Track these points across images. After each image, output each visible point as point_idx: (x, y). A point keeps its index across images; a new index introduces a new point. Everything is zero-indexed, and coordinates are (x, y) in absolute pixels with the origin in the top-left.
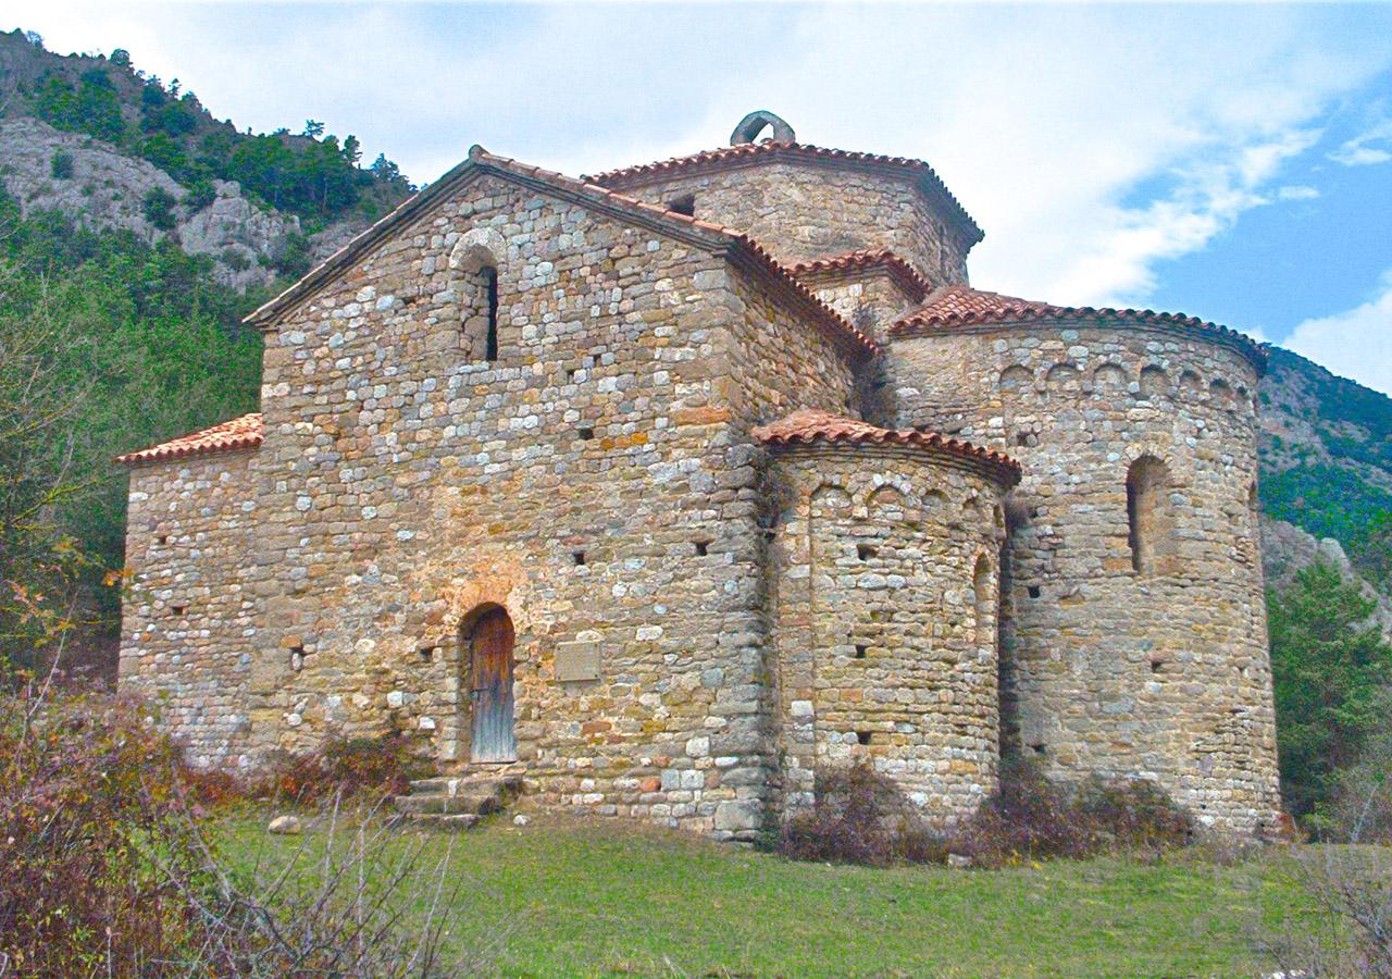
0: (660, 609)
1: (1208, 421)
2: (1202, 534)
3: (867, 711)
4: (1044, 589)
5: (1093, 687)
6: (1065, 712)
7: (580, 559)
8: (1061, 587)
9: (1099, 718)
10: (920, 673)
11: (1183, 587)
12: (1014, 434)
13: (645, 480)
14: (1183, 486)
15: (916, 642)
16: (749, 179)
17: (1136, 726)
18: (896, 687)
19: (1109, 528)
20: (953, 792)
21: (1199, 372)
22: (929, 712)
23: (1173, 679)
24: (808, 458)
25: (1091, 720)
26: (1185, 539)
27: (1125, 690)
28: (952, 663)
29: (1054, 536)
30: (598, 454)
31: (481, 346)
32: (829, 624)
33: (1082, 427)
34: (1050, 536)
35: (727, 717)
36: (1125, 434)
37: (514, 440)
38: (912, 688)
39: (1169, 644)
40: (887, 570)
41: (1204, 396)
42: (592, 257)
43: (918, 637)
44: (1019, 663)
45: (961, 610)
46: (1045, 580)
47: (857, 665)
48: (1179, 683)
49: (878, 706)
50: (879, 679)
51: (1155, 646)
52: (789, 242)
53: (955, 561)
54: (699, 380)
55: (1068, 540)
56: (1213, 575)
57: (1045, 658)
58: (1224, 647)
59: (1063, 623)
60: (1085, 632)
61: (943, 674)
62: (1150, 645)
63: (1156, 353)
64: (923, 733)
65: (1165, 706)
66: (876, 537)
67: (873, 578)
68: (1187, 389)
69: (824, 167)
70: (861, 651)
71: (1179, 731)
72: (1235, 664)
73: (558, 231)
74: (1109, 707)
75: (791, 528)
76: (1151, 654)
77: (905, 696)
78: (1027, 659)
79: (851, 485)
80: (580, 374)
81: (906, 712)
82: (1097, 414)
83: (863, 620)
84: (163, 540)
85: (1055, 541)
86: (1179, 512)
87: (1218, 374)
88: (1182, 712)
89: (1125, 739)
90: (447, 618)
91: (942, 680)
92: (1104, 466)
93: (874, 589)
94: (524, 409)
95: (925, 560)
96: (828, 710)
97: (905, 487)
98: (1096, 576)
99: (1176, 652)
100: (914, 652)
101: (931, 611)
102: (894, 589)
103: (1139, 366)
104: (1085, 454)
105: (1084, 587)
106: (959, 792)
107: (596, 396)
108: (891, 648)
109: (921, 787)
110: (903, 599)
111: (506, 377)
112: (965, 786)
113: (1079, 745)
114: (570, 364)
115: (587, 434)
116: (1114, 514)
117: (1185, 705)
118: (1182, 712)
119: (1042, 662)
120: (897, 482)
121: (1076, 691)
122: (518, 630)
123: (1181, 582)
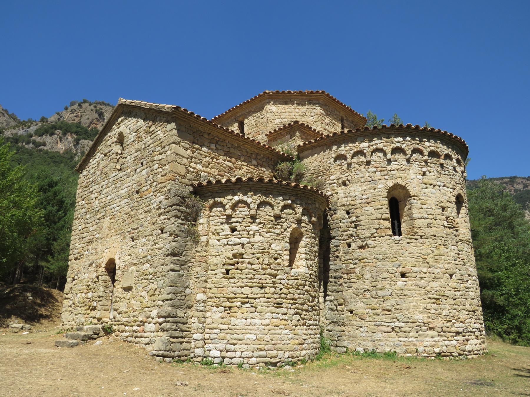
0: (149, 257)
1: (429, 168)
2: (426, 216)
3: (228, 298)
4: (353, 244)
5: (373, 284)
6: (361, 296)
8: (359, 243)
9: (376, 298)
10: (255, 280)
11: (417, 239)
12: (340, 181)
13: (150, 207)
14: (414, 196)
18: (242, 287)
19: (379, 216)
20: (272, 334)
21: (422, 148)
22: (259, 298)
25: (373, 299)
26: (416, 219)
27: (387, 286)
28: (275, 276)
29: (357, 221)
33: (367, 175)
34: (355, 222)
35: (163, 301)
36: (386, 177)
38: (251, 287)
39: (408, 265)
40: (240, 236)
41: (426, 158)
43: (254, 264)
44: (343, 275)
45: (281, 252)
46: (353, 240)
47: (225, 278)
49: (234, 296)
50: (235, 284)
52: (271, 125)
53: (278, 231)
56: (432, 233)
58: (440, 265)
60: (369, 261)
61: (268, 281)
62: (400, 266)
63: (399, 142)
66: (237, 222)
70: (228, 272)
71: (415, 304)
73: (137, 121)
75: (201, 221)
76: (400, 270)
77: (246, 290)
78: (346, 274)
81: (247, 298)
82: (374, 169)
83: (229, 258)
86: (413, 207)
88: (416, 295)
89: (389, 308)
91: (267, 283)
92: (377, 190)
95: (260, 231)
96: (212, 298)
97: (249, 200)
98: (375, 237)
99: (413, 269)
100: (252, 271)
103: (391, 147)
105: (369, 242)
106: (275, 334)
108: (241, 270)
109: (252, 332)
110: (248, 248)
112: (279, 331)
113: (367, 311)
114: (135, 168)
115: (138, 192)
117: (417, 292)
118: (416, 295)
119: (352, 275)
120: (245, 198)
121: (366, 287)
122: (117, 268)
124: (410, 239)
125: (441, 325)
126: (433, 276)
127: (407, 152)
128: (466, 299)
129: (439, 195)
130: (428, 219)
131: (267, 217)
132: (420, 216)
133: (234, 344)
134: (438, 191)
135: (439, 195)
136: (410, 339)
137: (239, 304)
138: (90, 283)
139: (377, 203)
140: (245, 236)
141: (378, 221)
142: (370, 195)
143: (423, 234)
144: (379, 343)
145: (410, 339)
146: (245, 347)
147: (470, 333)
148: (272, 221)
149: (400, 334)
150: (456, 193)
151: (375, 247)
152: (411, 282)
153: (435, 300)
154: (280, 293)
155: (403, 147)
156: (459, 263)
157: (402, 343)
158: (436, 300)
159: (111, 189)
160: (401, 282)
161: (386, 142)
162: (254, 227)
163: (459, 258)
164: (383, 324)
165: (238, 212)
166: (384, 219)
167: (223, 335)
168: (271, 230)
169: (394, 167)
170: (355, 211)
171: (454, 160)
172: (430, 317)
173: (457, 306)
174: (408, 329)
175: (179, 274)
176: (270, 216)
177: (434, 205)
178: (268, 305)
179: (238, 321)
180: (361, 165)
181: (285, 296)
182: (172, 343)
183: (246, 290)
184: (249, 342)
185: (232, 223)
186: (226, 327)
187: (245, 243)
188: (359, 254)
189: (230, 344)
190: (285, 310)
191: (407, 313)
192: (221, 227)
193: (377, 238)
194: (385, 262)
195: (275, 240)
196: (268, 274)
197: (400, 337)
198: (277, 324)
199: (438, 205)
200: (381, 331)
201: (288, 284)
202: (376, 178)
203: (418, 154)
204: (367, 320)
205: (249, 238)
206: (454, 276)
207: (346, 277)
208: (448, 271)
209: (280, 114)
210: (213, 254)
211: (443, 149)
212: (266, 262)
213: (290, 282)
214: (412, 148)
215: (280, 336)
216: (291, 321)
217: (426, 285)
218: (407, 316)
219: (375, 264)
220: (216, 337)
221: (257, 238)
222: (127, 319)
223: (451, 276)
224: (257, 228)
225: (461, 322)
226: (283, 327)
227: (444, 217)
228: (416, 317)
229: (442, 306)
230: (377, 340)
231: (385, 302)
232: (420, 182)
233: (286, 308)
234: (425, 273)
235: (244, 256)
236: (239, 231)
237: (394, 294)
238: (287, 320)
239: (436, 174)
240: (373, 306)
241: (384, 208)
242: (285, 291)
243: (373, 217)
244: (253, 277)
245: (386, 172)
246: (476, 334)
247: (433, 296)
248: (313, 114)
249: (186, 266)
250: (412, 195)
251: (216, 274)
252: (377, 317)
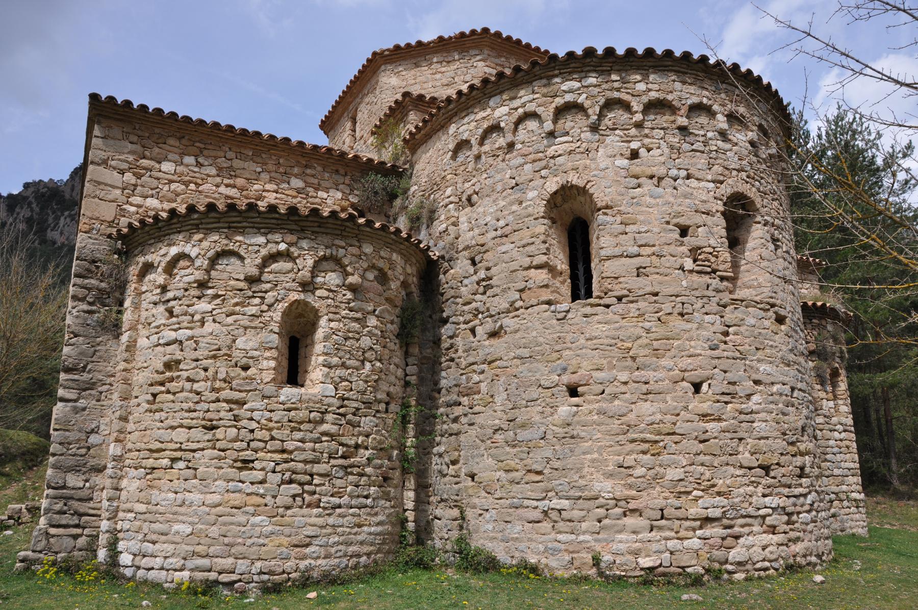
1: (647, 141)
2: (635, 250)
3: (151, 450)
4: (479, 330)
6: (489, 442)
8: (489, 325)
9: (514, 446)
11: (608, 306)
14: (607, 207)
15: (196, 386)
17: (549, 454)
18: (173, 428)
19: (526, 261)
20: (225, 524)
22: (203, 449)
23: (590, 402)
25: (508, 449)
26: (609, 258)
27: (537, 418)
28: (241, 403)
33: (508, 176)
34: (483, 280)
36: (543, 173)
39: (584, 367)
41: (638, 117)
43: (198, 381)
48: (596, 406)
49: (159, 445)
50: (162, 422)
53: (253, 310)
56: (649, 289)
57: (479, 392)
58: (665, 362)
59: (489, 358)
61: (222, 414)
62: (565, 369)
63: (571, 91)
64: (196, 469)
65: (577, 430)
66: (175, 299)
68: (616, 116)
71: (595, 456)
72: (683, 380)
74: (523, 435)
76: (566, 379)
77: (180, 435)
78: (467, 395)
81: (180, 449)
82: (520, 160)
87: (653, 95)
88: (599, 435)
89: (539, 468)
91: (221, 419)
92: (524, 205)
98: (517, 310)
99: (597, 375)
100: (191, 395)
102: (181, 341)
103: (554, 105)
105: (508, 322)
106: (232, 524)
108: (174, 394)
112: (242, 519)
113: (498, 473)
117: (603, 428)
118: (599, 435)
119: (476, 397)
120: (188, 249)
121: (497, 422)
123: (602, 302)
124: (592, 305)
125: (661, 502)
126: (644, 388)
127: (590, 111)
128: (741, 439)
129: (672, 199)
130: (639, 255)
131: (232, 282)
132: (618, 251)
133: (154, 543)
134: (669, 190)
135: (672, 199)
136: (581, 538)
137: (166, 462)
139: (526, 233)
140: (185, 324)
141: (525, 273)
142: (510, 218)
143: (625, 292)
144: (517, 544)
145: (581, 538)
146: (170, 548)
147: (748, 520)
148: (241, 290)
149: (561, 525)
150: (726, 190)
151: (516, 331)
152: (589, 405)
153: (646, 446)
154: (247, 440)
155: (579, 101)
156: (726, 354)
157: (563, 547)
158: (652, 446)
161: (544, 96)
162: (203, 306)
163: (725, 343)
165: (178, 278)
166: (538, 267)
168: (237, 308)
169: (560, 149)
170: (485, 256)
171: (720, 117)
172: (630, 487)
173: (708, 457)
174: (576, 514)
175: (75, 408)
176: (238, 280)
177: (656, 223)
178: (221, 463)
179: (164, 497)
180: (498, 156)
181: (261, 445)
182: (53, 536)
183: (180, 435)
184: (177, 539)
185: (168, 301)
186: (141, 508)
188: (487, 351)
189: (148, 542)
190: (259, 475)
191: (576, 477)
193: (522, 310)
195: (246, 328)
196: (228, 401)
197: (560, 532)
198: (236, 503)
199: (668, 223)
200: (520, 519)
201: (270, 420)
203: (621, 112)
204: (496, 496)
205: (191, 328)
206: (705, 387)
207: (466, 403)
208: (686, 374)
210: (140, 365)
211: (686, 93)
212: (221, 375)
213: (276, 416)
214: (603, 100)
215: (243, 529)
216: (274, 497)
217: (624, 410)
218: (576, 484)
219: (514, 371)
221: (209, 327)
223: (697, 387)
224: (209, 307)
225: (719, 494)
226: (251, 509)
227: (684, 249)
228: (597, 486)
229: (665, 458)
230: (512, 539)
231: (531, 455)
233: (263, 469)
234: (626, 383)
235: (181, 366)
237: (549, 436)
238: (262, 496)
239: (667, 151)
240: (507, 465)
241: (538, 241)
242: (265, 435)
243: (514, 265)
244: (193, 408)
245: (543, 163)
246: (769, 520)
247: (642, 436)
249: (93, 392)
250: (599, 205)
252: (515, 488)
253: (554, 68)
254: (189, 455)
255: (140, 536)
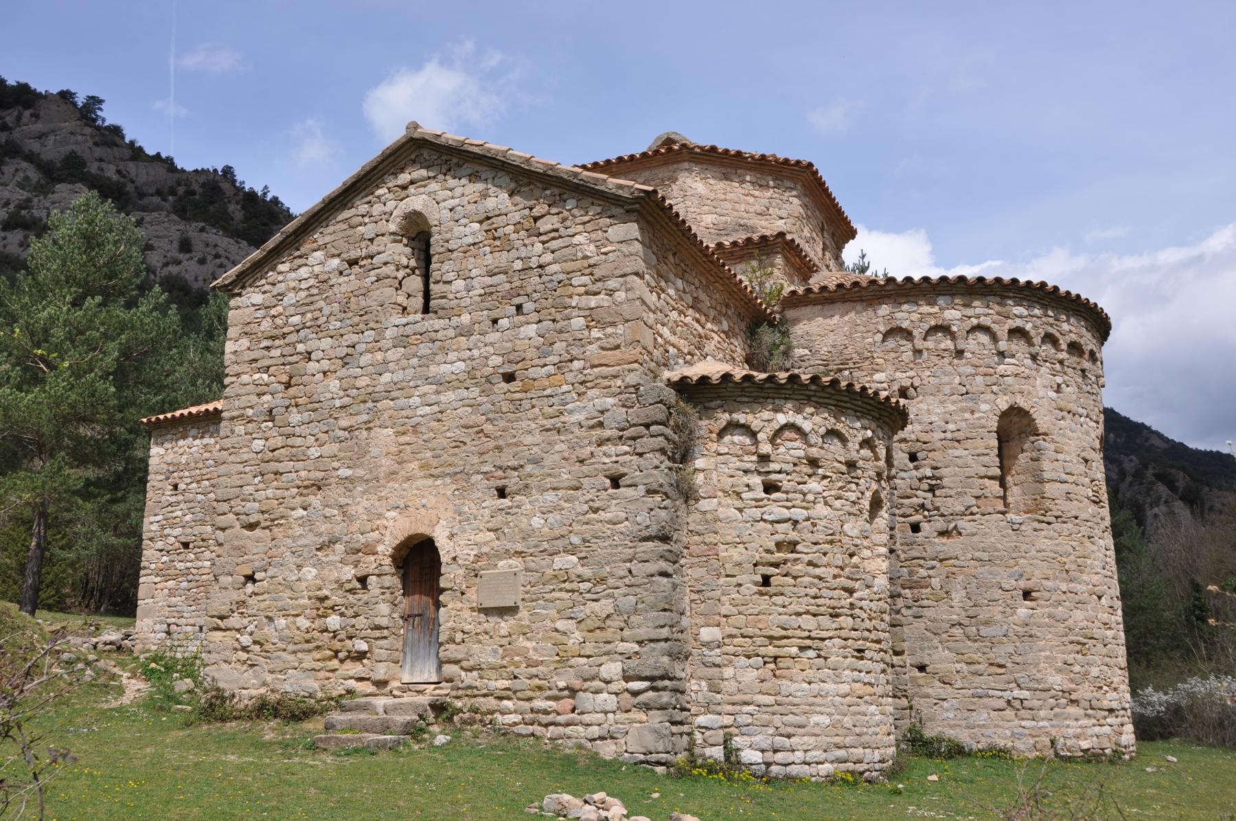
0: (575, 540)
1: (1066, 378)
2: (1064, 477)
3: (771, 638)
4: (925, 526)
5: (970, 613)
6: (945, 635)
7: (502, 493)
8: (940, 524)
11: (1049, 523)
13: (562, 419)
15: (818, 571)
16: (660, 176)
17: (1011, 649)
18: (799, 614)
20: (854, 714)
21: (1057, 335)
22: (831, 638)
23: (1042, 607)
24: (715, 399)
25: (969, 643)
27: (999, 617)
29: (933, 477)
30: (517, 396)
31: (419, 301)
32: (736, 554)
35: (640, 643)
36: (995, 388)
37: (442, 384)
38: (815, 615)
40: (789, 504)
41: (1063, 355)
42: (517, 217)
44: (903, 592)
45: (859, 542)
46: (925, 517)
47: (761, 594)
49: (784, 633)
51: (1026, 576)
53: (853, 496)
54: (613, 324)
55: (946, 482)
56: (1074, 513)
57: (927, 587)
58: (1085, 577)
60: (962, 564)
61: (843, 602)
62: (1021, 576)
63: (1020, 317)
64: (826, 658)
66: (780, 472)
67: (780, 512)
68: (1046, 350)
69: (722, 165)
70: (766, 581)
71: (1048, 653)
73: (485, 195)
74: (984, 631)
76: (1023, 584)
77: (808, 622)
78: (910, 588)
79: (755, 424)
80: (504, 323)
81: (809, 637)
82: (970, 370)
83: (768, 551)
84: (175, 487)
85: (934, 482)
87: (1073, 337)
88: (1050, 636)
89: (1003, 662)
90: (380, 548)
92: (977, 415)
93: (778, 522)
94: (452, 356)
95: (825, 494)
97: (807, 426)
98: (972, 514)
99: (1045, 582)
100: (816, 581)
101: (831, 542)
103: (1007, 327)
104: (959, 405)
105: (963, 524)
107: (518, 342)
108: (795, 578)
111: (436, 328)
112: (863, 708)
113: (958, 666)
114: (494, 314)
115: (509, 378)
116: (986, 459)
117: (1052, 629)
118: (1050, 636)
119: (924, 591)
121: (955, 617)
122: (444, 559)
123: (1045, 519)
124: (1040, 522)
125: (1088, 695)
127: (1035, 340)
131: (836, 464)
132: (1053, 476)
133: (789, 736)
136: (1041, 724)
137: (795, 650)
138: (325, 592)
140: (798, 502)
141: (981, 481)
143: (1059, 513)
144: (983, 731)
145: (1041, 724)
146: (812, 740)
149: (1022, 713)
151: (974, 535)
153: (1079, 647)
157: (1027, 732)
159: (391, 355)
160: (1023, 611)
161: (998, 314)
162: (814, 485)
164: (991, 692)
165: (782, 449)
166: (991, 478)
167: (766, 716)
169: (1010, 369)
170: (930, 455)
172: (1072, 680)
174: (1036, 703)
179: (796, 687)
184: (817, 730)
185: (769, 473)
186: (769, 700)
187: (800, 518)
188: (938, 549)
189: (781, 735)
191: (1034, 671)
192: (746, 479)
193: (978, 516)
194: (995, 568)
197: (1023, 719)
200: (986, 707)
202: (975, 389)
203: (1049, 346)
207: (909, 596)
209: (714, 203)
210: (729, 539)
217: (1066, 616)
220: (750, 721)
222: (506, 683)
228: (1051, 679)
230: (978, 726)
232: (1054, 405)
235: (799, 547)
236: (787, 492)
245: (993, 379)
248: (783, 213)
250: (1037, 429)
251: (740, 585)
252: (978, 679)
253: (1010, 290)
254: (817, 644)
255: (771, 731)
